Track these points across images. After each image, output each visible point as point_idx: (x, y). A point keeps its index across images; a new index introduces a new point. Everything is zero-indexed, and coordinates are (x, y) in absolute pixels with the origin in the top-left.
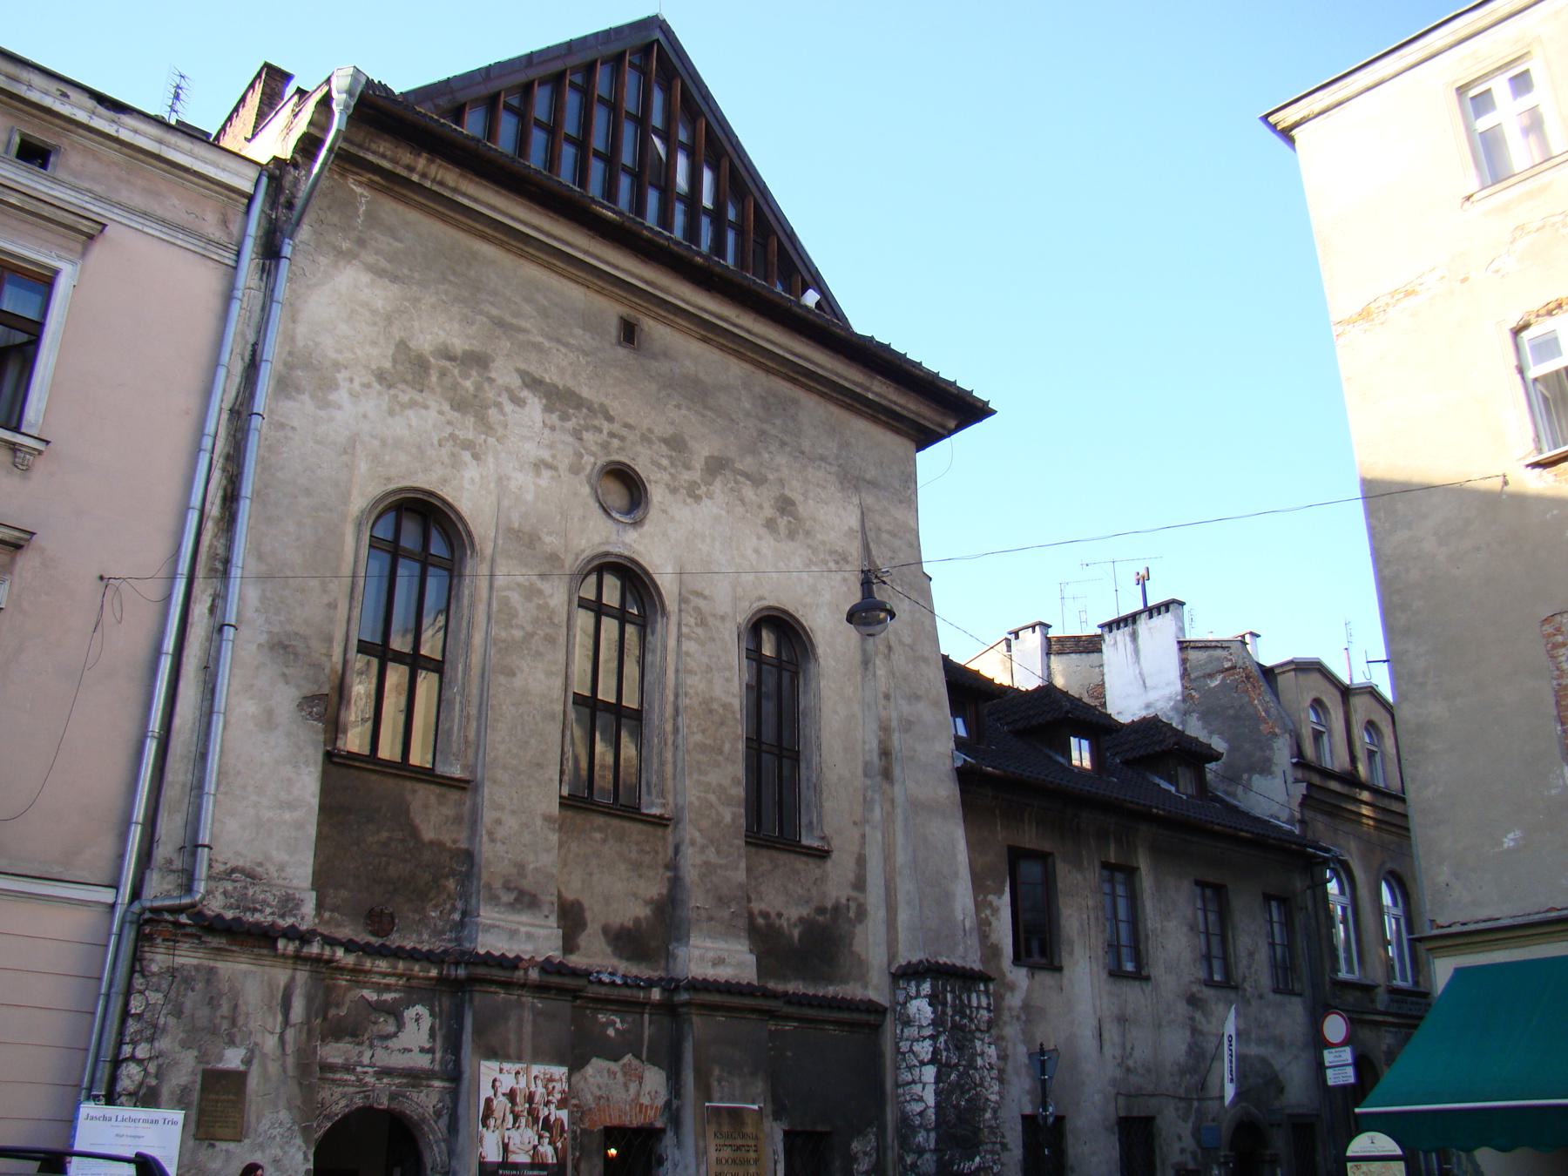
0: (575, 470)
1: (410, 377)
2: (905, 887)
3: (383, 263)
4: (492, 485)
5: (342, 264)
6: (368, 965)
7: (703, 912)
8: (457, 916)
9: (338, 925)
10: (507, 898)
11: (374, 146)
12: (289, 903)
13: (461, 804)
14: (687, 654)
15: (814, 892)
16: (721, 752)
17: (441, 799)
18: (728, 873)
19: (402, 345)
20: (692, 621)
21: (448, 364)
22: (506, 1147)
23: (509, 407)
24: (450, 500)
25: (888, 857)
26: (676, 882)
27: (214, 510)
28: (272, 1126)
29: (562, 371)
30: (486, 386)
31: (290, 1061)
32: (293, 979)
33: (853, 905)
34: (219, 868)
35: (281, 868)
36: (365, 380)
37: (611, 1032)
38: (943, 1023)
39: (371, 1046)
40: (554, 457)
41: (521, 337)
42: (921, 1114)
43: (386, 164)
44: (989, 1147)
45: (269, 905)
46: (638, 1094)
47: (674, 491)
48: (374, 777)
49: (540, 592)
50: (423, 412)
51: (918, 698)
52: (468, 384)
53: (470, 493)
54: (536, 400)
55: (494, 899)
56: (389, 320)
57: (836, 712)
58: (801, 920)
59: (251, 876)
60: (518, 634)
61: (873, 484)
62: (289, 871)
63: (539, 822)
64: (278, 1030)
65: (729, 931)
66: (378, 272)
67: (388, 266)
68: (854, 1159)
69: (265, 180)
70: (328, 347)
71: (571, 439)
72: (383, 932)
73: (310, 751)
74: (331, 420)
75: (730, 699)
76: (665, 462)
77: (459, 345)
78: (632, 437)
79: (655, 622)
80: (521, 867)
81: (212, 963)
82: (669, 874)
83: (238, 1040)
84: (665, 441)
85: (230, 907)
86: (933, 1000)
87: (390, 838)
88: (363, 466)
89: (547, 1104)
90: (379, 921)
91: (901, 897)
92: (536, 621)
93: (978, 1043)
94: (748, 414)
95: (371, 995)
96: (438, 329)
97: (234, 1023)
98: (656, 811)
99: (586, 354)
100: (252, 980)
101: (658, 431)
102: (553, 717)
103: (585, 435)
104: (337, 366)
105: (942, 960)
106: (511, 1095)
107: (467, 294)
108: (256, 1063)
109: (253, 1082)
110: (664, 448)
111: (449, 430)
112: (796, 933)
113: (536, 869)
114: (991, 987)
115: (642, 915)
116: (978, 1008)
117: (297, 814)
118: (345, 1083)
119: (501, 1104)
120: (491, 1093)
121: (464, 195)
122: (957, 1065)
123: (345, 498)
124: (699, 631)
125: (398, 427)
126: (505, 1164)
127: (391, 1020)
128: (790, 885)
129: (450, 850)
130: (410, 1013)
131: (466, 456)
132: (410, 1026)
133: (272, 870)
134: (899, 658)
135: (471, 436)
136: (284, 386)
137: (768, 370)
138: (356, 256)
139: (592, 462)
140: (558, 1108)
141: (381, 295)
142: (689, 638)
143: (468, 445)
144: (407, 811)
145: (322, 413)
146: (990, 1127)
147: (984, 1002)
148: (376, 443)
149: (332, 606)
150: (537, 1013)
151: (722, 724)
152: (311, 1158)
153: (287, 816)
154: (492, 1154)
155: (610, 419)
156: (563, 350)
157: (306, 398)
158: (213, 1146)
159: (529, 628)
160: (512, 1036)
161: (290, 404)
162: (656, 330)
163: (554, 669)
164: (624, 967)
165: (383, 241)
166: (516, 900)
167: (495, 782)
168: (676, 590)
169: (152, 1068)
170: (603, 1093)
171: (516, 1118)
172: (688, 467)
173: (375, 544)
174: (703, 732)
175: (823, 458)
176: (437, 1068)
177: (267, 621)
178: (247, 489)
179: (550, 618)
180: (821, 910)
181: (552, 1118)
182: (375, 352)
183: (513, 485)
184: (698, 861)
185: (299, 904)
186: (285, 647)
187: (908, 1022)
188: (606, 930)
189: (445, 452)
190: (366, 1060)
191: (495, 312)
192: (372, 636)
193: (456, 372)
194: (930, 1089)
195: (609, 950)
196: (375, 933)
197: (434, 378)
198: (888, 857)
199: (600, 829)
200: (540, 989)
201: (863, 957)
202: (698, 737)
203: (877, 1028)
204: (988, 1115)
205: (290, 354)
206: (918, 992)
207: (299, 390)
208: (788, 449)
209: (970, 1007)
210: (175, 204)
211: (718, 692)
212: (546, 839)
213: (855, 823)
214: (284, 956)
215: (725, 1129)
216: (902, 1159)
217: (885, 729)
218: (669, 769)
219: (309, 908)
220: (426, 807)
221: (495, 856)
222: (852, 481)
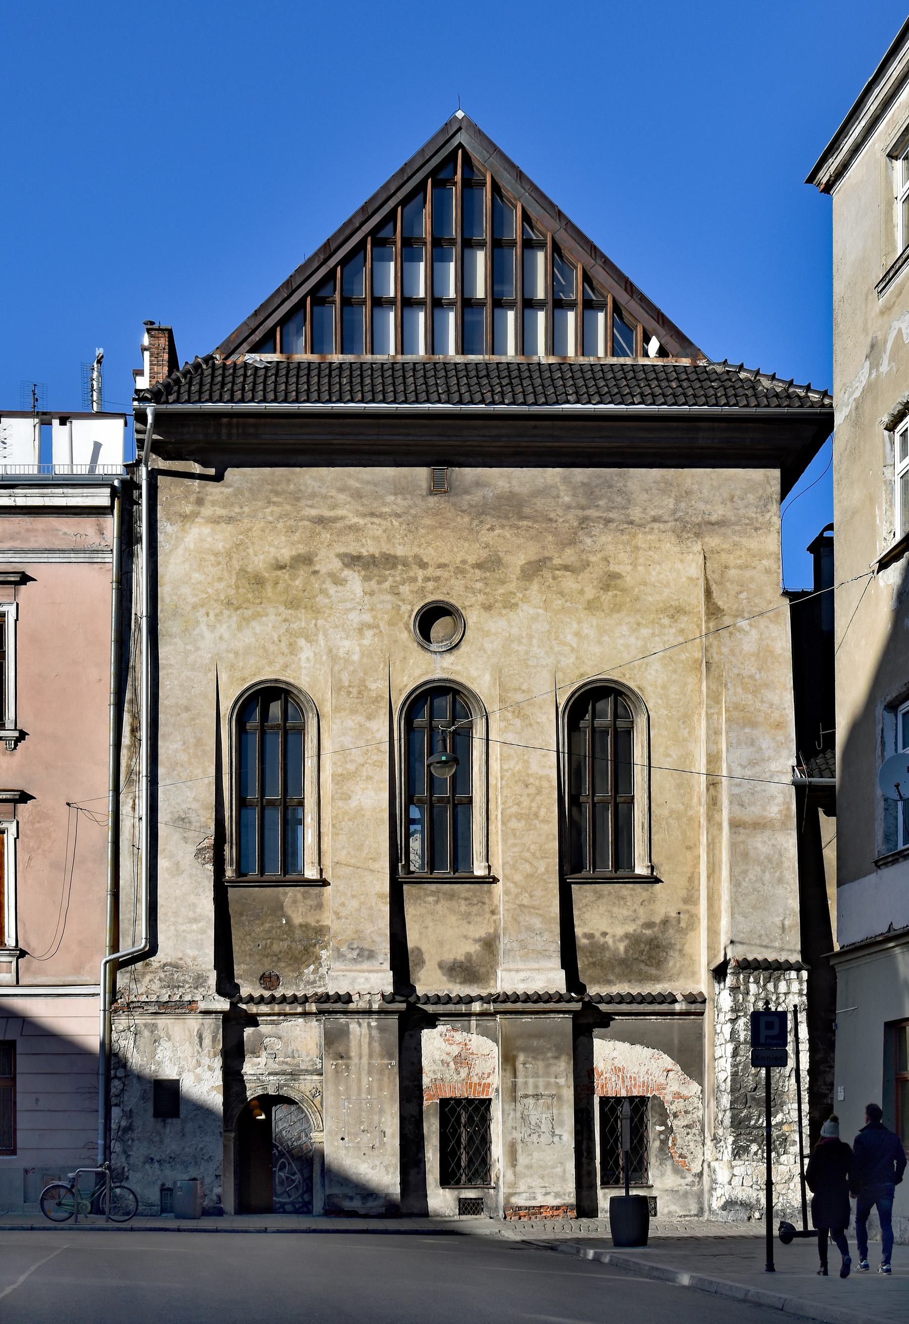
1: (250, 596)
4: (324, 658)
5: (187, 526)
16: (536, 815)
17: (305, 896)
21: (279, 573)
23: (332, 589)
24: (291, 681)
29: (376, 539)
35: (194, 959)
36: (217, 611)
40: (375, 617)
41: (339, 525)
45: (187, 982)
47: (488, 608)
50: (264, 619)
51: (754, 724)
54: (356, 574)
56: (229, 556)
57: (668, 755)
58: (627, 936)
59: (176, 966)
60: (351, 767)
61: (721, 523)
66: (215, 521)
71: (389, 597)
75: (542, 772)
76: (479, 585)
77: (286, 554)
81: (153, 1021)
84: (479, 566)
87: (272, 927)
94: (569, 507)
99: (398, 516)
101: (472, 559)
107: (288, 507)
110: (477, 571)
111: (285, 626)
112: (622, 947)
117: (201, 925)
125: (247, 638)
128: (615, 910)
129: (314, 928)
131: (302, 642)
135: (303, 624)
138: (196, 514)
144: (282, 907)
148: (231, 656)
153: (195, 927)
155: (423, 565)
156: (376, 520)
157: (177, 640)
159: (361, 760)
166: (358, 955)
168: (496, 692)
170: (439, 1076)
172: (503, 582)
174: (519, 804)
175: (655, 520)
182: (221, 586)
183: (341, 653)
186: (183, 819)
188: (441, 966)
189: (283, 644)
191: (314, 512)
193: (287, 577)
195: (445, 978)
197: (269, 590)
199: (433, 893)
202: (514, 809)
208: (613, 526)
211: (534, 768)
212: (380, 910)
220: (295, 902)
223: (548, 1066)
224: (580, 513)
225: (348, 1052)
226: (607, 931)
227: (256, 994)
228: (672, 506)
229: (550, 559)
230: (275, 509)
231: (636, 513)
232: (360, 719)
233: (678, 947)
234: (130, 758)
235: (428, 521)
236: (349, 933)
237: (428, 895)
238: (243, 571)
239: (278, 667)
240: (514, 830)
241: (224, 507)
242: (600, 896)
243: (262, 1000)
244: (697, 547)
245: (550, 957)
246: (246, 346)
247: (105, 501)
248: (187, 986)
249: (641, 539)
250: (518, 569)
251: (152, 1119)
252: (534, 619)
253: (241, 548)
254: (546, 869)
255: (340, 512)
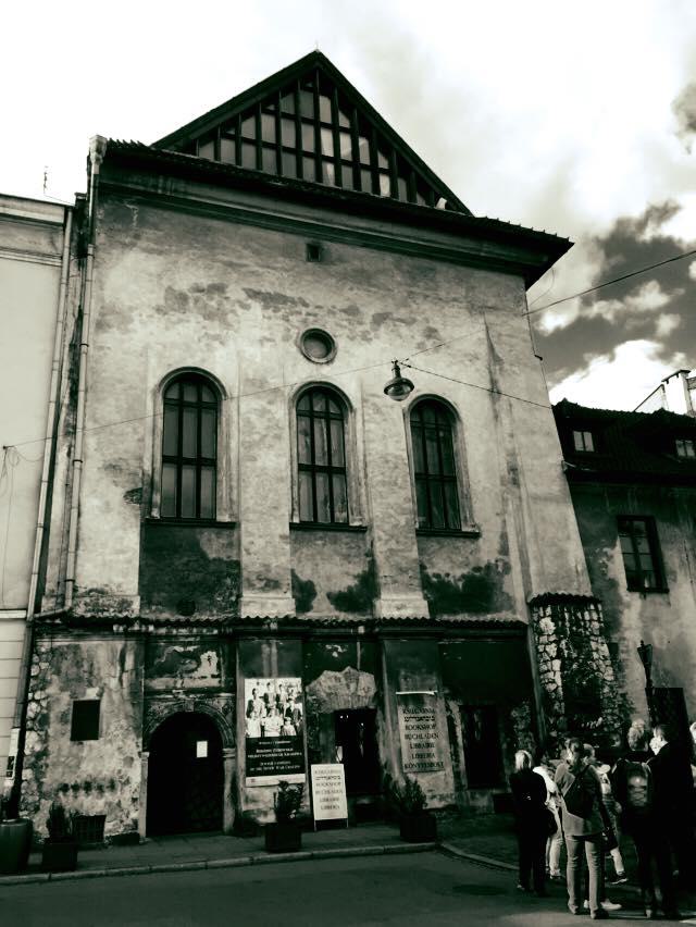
0: (286, 339)
1: (176, 306)
2: (532, 549)
3: (152, 245)
5: (127, 250)
6: (175, 632)
7: (389, 579)
8: (233, 599)
9: (161, 612)
10: (260, 584)
11: (130, 180)
12: (125, 604)
13: (230, 536)
14: (369, 431)
15: (471, 557)
16: (396, 484)
18: (406, 554)
19: (170, 289)
20: (371, 412)
21: (198, 294)
22: (263, 728)
23: (240, 311)
25: (520, 531)
26: (373, 564)
27: (66, 401)
28: (116, 729)
29: (273, 284)
30: (225, 302)
31: (126, 691)
32: (126, 646)
33: (500, 564)
34: (81, 591)
35: (119, 586)
37: (335, 654)
38: (564, 633)
39: (182, 677)
40: (271, 334)
41: (243, 270)
42: (555, 690)
43: (141, 188)
44: (609, 711)
46: (356, 689)
47: (352, 339)
48: (177, 529)
49: (269, 411)
50: (186, 325)
51: (533, 433)
52: (213, 303)
53: (220, 365)
54: (257, 304)
55: (251, 586)
56: (159, 276)
58: (463, 576)
59: (102, 592)
60: (256, 437)
62: (124, 587)
63: (277, 539)
64: (118, 675)
65: (409, 587)
67: (156, 247)
68: (514, 721)
69: (70, 214)
70: (125, 300)
71: (282, 322)
72: (191, 613)
73: (133, 520)
74: (132, 339)
75: (398, 453)
76: (345, 323)
77: (205, 282)
78: (321, 313)
79: (347, 416)
80: (267, 567)
82: (369, 559)
83: (94, 684)
84: (345, 311)
85: (89, 611)
86: (554, 618)
87: (189, 561)
88: (153, 361)
89: (289, 700)
90: (186, 607)
91: (531, 556)
92: (268, 428)
93: (593, 645)
95: (180, 649)
96: (190, 274)
97: (91, 673)
98: (357, 524)
99: (286, 271)
100: (100, 650)
101: (339, 306)
102: (281, 480)
103: (291, 318)
104: (131, 309)
105: (560, 593)
106: (265, 698)
108: (105, 695)
109: (104, 706)
110: (344, 316)
111: (204, 331)
112: (460, 584)
113: (277, 566)
114: (600, 607)
115: (353, 585)
116: (591, 621)
118: (167, 700)
119: (259, 704)
120: (252, 697)
121: (192, 195)
122: (577, 659)
123: (144, 379)
124: (377, 416)
125: (173, 336)
126: (263, 738)
127: (194, 662)
128: (454, 556)
130: (204, 657)
131: (216, 344)
132: (205, 663)
133: (114, 588)
134: (519, 412)
136: (101, 326)
137: (411, 255)
138: (134, 245)
139: (297, 330)
140: (296, 702)
141: (153, 264)
142: (369, 421)
143: (216, 337)
145: (124, 337)
146: (609, 698)
147: (595, 616)
149: (142, 440)
150: (279, 648)
151: (396, 467)
152: (140, 745)
153: (121, 557)
154: (254, 733)
155: (306, 305)
156: (273, 271)
157: (115, 329)
158: (82, 743)
159: (264, 433)
160: (265, 663)
161: (105, 335)
162: (333, 248)
163: (281, 452)
164: (343, 616)
165: (150, 233)
166: (266, 585)
167: (248, 521)
168: (359, 395)
169: (44, 704)
171: (269, 710)
172: (361, 323)
173: (167, 403)
176: (223, 686)
177: (103, 455)
178: (82, 386)
179: (277, 425)
180: (477, 569)
181: (292, 709)
182: (154, 296)
183: (247, 355)
184: (384, 548)
185: (130, 604)
186: (114, 467)
187: (541, 633)
188: (329, 596)
189: (202, 344)
190: (179, 686)
191: (226, 259)
192: (172, 452)
193: (205, 298)
194: (558, 674)
195: (332, 607)
196: (182, 614)
197: (191, 304)
198: (520, 531)
199: (321, 538)
200: (278, 634)
201: (511, 595)
202: (380, 478)
203: (524, 638)
204: (606, 690)
205: (102, 308)
206: (545, 613)
207: (109, 326)
208: (429, 299)
209: (583, 620)
210: (22, 239)
213: (498, 514)
214: (118, 634)
215: (411, 707)
216: (547, 721)
217: (512, 454)
218: (364, 499)
219: (136, 605)
220: (209, 540)
221: (250, 564)
222: (476, 309)
223: (423, 680)
224: (408, 288)
225: (262, 667)
226: (451, 572)
227: (173, 619)
228: (464, 294)
229: (391, 313)
230: (196, 251)
231: (442, 294)
232: (263, 403)
233: (499, 586)
234: (68, 414)
235: (309, 278)
236: (257, 568)
237: (316, 539)
238: (170, 288)
239: (197, 359)
240: (380, 492)
241: (156, 244)
242: (442, 547)
243: (178, 625)
244: (482, 321)
245: (415, 590)
246: (173, 147)
247: (61, 220)
248: (112, 610)
249: (447, 310)
250: (371, 318)
251: (69, 743)
252: (384, 350)
253: (169, 273)
254: (407, 523)
255: (244, 262)
